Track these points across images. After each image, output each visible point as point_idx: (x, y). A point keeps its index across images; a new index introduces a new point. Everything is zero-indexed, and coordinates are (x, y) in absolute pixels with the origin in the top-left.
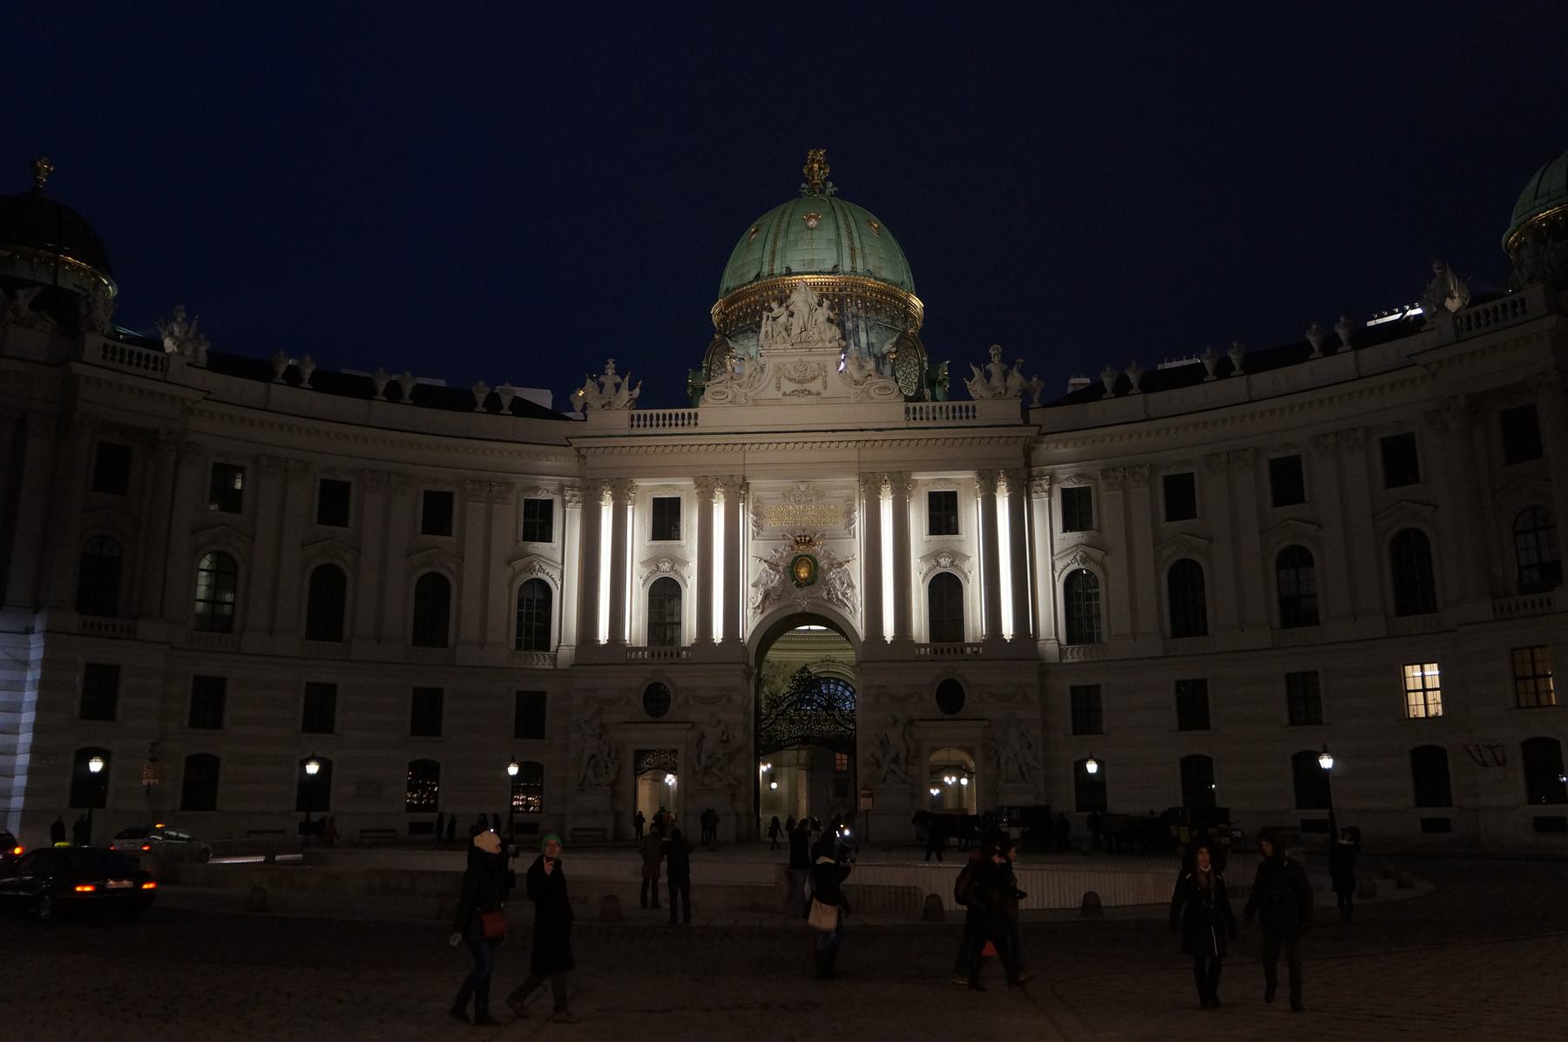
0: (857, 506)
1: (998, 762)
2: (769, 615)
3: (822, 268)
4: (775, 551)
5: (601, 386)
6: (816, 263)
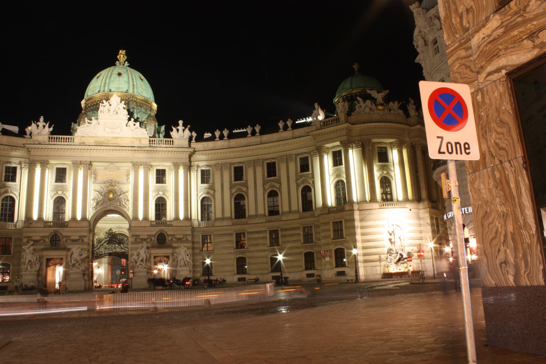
1: (177, 261)
2: (99, 210)
3: (122, 90)
4: (101, 188)
5: (38, 126)
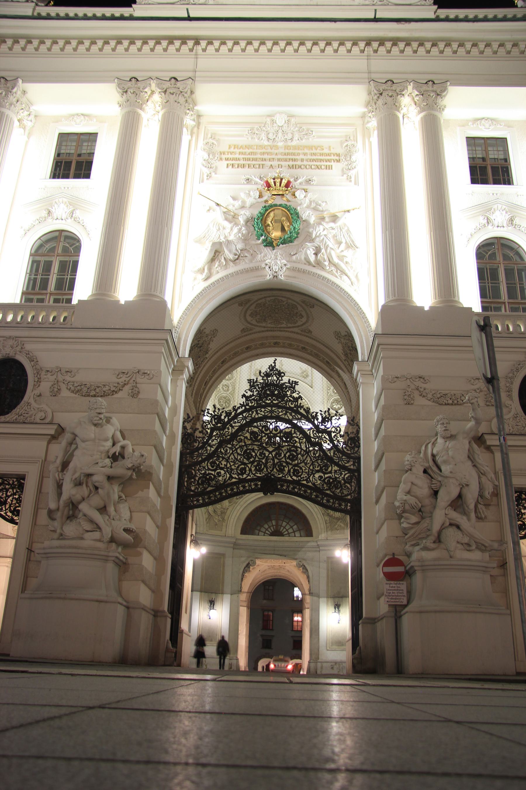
0: (360, 144)
4: (234, 199)
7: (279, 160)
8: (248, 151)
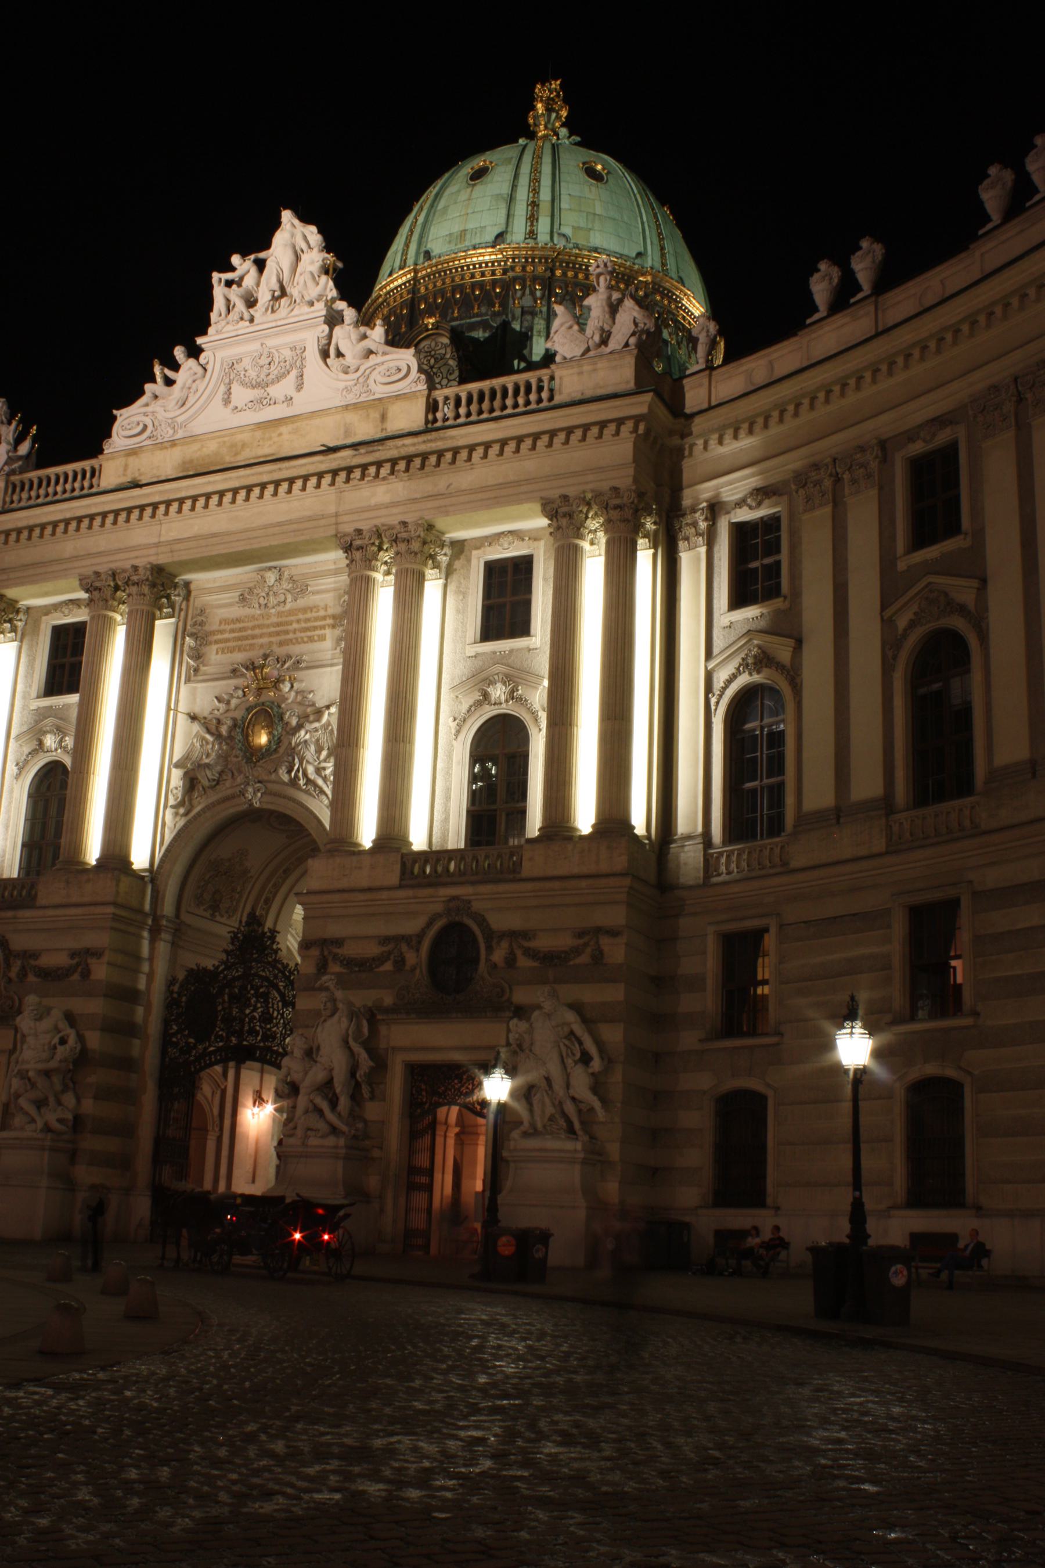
6: (468, 236)
7: (270, 635)
8: (238, 625)
